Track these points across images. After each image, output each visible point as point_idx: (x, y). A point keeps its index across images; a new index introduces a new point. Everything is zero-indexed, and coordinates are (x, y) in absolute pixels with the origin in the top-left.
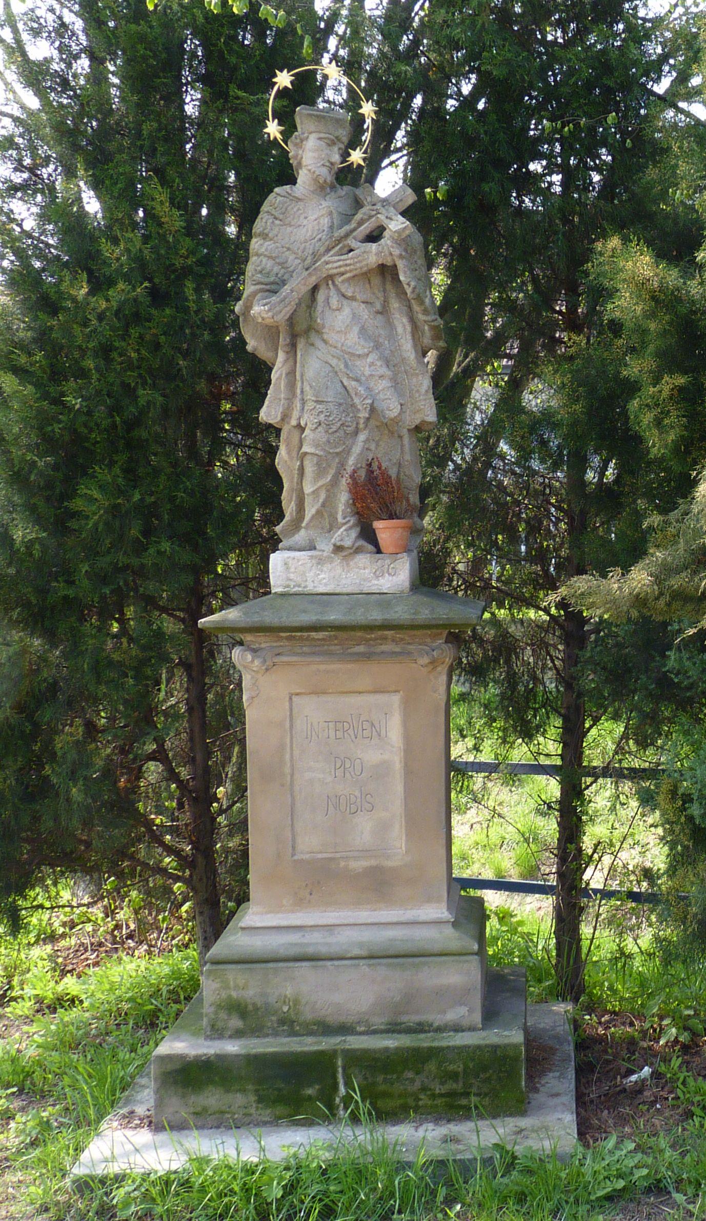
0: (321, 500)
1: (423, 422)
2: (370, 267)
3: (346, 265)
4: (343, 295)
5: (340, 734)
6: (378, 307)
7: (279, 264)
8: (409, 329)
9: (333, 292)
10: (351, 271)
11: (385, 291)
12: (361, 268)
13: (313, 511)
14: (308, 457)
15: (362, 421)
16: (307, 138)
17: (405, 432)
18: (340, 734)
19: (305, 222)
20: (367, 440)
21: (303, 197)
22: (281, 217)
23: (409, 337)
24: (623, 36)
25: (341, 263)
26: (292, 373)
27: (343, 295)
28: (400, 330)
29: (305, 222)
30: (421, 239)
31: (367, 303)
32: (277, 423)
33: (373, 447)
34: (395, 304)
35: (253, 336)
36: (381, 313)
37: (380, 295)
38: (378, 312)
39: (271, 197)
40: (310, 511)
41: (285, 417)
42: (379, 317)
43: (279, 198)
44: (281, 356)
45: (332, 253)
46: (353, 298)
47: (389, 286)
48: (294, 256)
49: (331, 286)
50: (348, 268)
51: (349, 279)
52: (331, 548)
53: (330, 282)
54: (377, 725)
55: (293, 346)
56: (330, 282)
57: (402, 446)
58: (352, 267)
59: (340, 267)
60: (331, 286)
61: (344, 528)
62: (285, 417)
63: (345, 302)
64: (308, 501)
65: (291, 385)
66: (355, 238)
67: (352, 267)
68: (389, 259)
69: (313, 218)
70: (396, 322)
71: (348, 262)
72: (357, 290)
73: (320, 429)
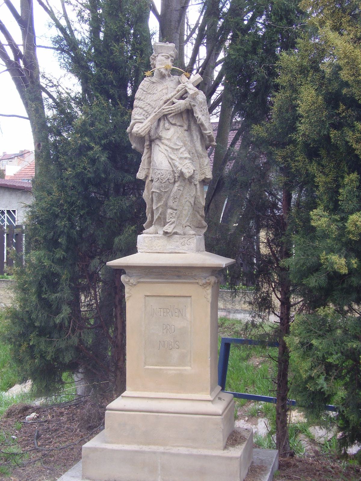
0: (160, 212)
1: (205, 178)
2: (182, 111)
3: (172, 110)
4: (171, 123)
5: (165, 314)
6: (186, 127)
7: (145, 111)
8: (199, 137)
9: (166, 122)
10: (173, 113)
11: (189, 121)
12: (178, 111)
13: (157, 217)
14: (154, 193)
15: (177, 177)
16: (158, 56)
17: (197, 183)
18: (165, 314)
19: (156, 92)
20: (180, 186)
21: (156, 81)
22: (146, 90)
23: (199, 140)
24: (263, 30)
25: (169, 109)
26: (150, 157)
27: (171, 123)
28: (195, 138)
29: (156, 92)
30: (205, 97)
31: (181, 126)
32: (144, 179)
33: (182, 189)
34: (193, 127)
35: (134, 142)
36: (187, 131)
37: (187, 122)
38: (185, 130)
39: (143, 82)
40: (156, 217)
41: (147, 177)
42: (186, 132)
43: (146, 82)
44: (146, 151)
45: (166, 104)
46: (175, 125)
47: (191, 119)
48: (151, 107)
49: (166, 119)
50: (172, 111)
51: (173, 116)
52: (162, 232)
53: (165, 118)
54: (181, 311)
55: (150, 145)
56: (165, 118)
57: (196, 189)
58: (174, 111)
59: (169, 111)
60: (166, 119)
61: (168, 224)
62: (147, 177)
63: (172, 126)
64: (155, 212)
65: (149, 163)
66: (176, 98)
67: (174, 111)
68: (190, 107)
69: (159, 90)
70: (194, 135)
71: (172, 108)
72: (177, 121)
73: (159, 181)
